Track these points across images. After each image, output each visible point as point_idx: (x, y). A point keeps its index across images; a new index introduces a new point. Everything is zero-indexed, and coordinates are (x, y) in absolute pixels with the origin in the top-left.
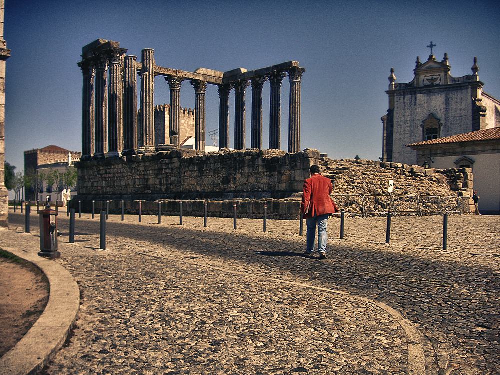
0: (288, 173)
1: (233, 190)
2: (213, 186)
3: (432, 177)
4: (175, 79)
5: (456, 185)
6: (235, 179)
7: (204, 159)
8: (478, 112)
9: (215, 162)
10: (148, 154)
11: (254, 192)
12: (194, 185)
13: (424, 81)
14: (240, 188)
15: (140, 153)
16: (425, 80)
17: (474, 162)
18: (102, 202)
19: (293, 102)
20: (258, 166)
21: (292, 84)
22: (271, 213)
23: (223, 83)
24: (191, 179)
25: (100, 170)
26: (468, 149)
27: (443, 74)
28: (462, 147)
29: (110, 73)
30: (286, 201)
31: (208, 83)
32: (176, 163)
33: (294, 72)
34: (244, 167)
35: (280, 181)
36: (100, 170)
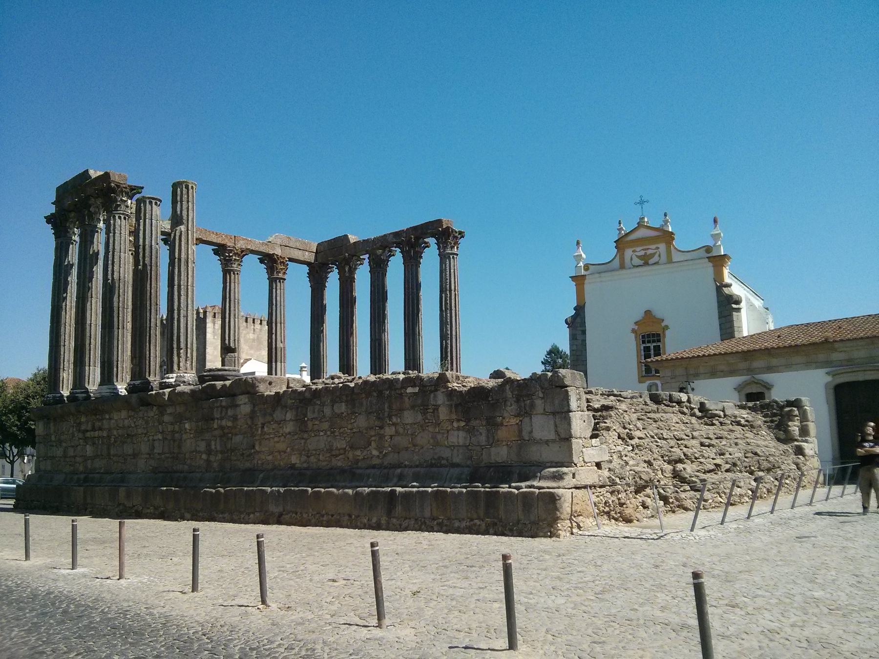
0: (514, 421)
1: (376, 461)
2: (328, 455)
3: (736, 417)
4: (231, 251)
5: (787, 431)
6: (382, 437)
7: (307, 395)
8: (727, 305)
9: (333, 402)
10: (182, 388)
11: (430, 470)
12: (285, 452)
13: (631, 259)
14: (392, 458)
15: (163, 386)
16: (634, 257)
17: (772, 386)
18: (82, 488)
19: (446, 289)
20: (436, 408)
21: (444, 258)
22: (479, 518)
23: (316, 259)
24: (276, 439)
25: (80, 424)
26: (758, 364)
27: (662, 247)
28: (746, 360)
29: (108, 233)
30: (518, 488)
31: (291, 260)
32: (244, 406)
33: (445, 236)
34: (401, 410)
35: (493, 442)
36: (80, 424)
